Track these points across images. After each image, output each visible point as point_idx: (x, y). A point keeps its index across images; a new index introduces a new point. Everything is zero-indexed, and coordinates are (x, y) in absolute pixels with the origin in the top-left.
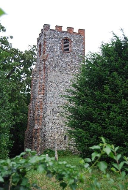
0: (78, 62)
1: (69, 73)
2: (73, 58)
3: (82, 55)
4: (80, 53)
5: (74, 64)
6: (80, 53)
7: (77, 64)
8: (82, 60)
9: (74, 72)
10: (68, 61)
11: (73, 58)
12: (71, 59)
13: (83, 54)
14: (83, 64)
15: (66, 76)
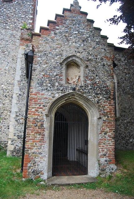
0: (24, 14)
1: (7, 27)
2: (17, 9)
3: (31, 6)
4: (28, 3)
5: (17, 16)
6: (28, 3)
7: (22, 16)
8: (30, 12)
9: (16, 27)
10: (8, 12)
11: (17, 9)
12: (14, 10)
13: (32, 5)
14: (32, 16)
15: (4, 31)
